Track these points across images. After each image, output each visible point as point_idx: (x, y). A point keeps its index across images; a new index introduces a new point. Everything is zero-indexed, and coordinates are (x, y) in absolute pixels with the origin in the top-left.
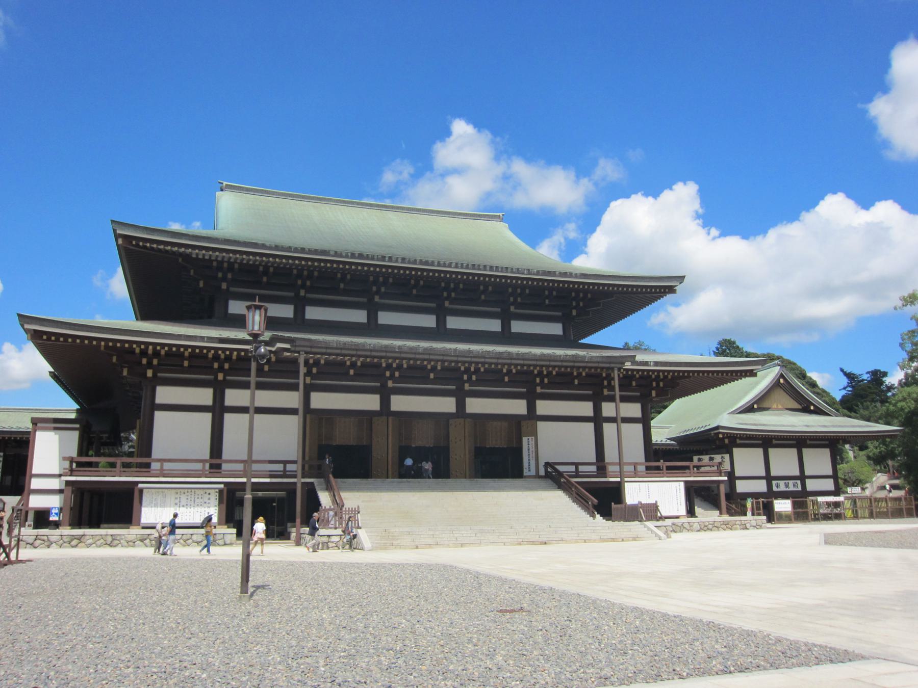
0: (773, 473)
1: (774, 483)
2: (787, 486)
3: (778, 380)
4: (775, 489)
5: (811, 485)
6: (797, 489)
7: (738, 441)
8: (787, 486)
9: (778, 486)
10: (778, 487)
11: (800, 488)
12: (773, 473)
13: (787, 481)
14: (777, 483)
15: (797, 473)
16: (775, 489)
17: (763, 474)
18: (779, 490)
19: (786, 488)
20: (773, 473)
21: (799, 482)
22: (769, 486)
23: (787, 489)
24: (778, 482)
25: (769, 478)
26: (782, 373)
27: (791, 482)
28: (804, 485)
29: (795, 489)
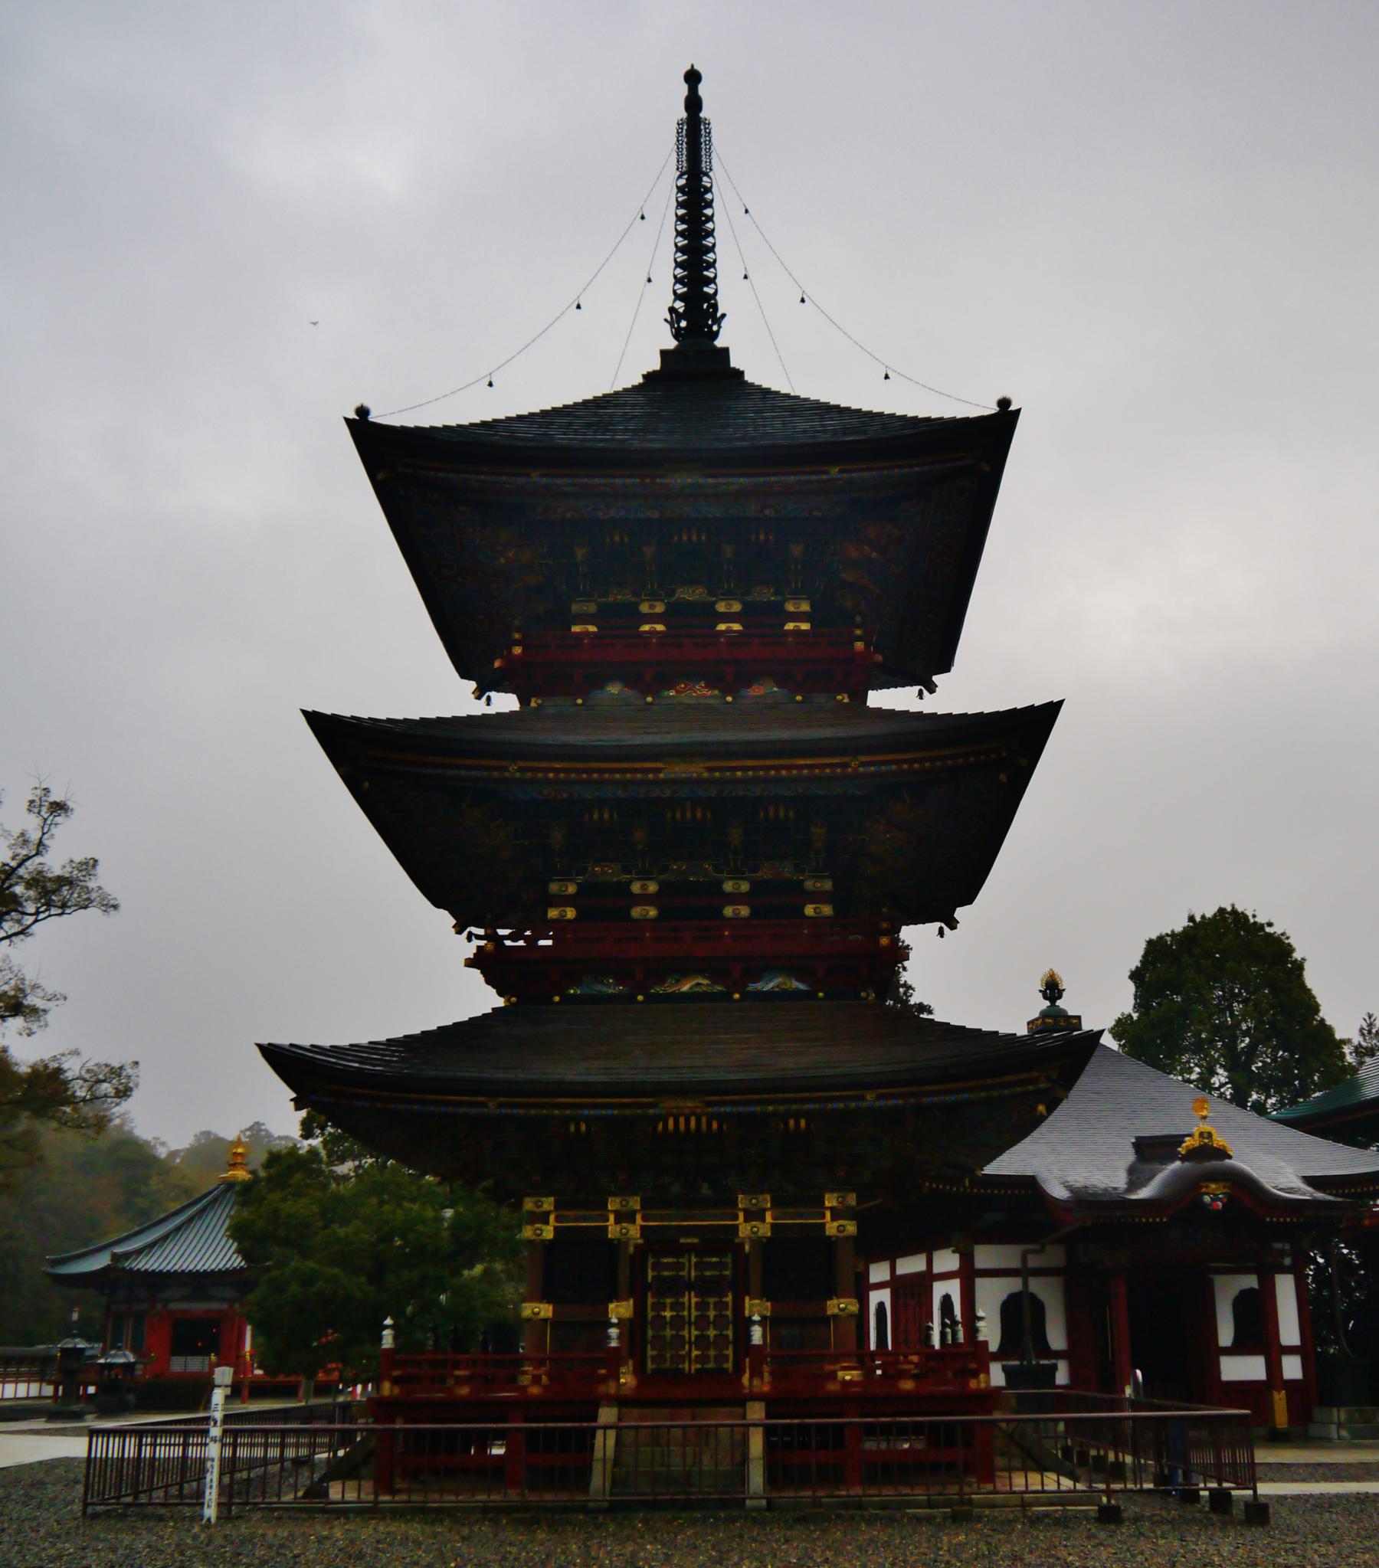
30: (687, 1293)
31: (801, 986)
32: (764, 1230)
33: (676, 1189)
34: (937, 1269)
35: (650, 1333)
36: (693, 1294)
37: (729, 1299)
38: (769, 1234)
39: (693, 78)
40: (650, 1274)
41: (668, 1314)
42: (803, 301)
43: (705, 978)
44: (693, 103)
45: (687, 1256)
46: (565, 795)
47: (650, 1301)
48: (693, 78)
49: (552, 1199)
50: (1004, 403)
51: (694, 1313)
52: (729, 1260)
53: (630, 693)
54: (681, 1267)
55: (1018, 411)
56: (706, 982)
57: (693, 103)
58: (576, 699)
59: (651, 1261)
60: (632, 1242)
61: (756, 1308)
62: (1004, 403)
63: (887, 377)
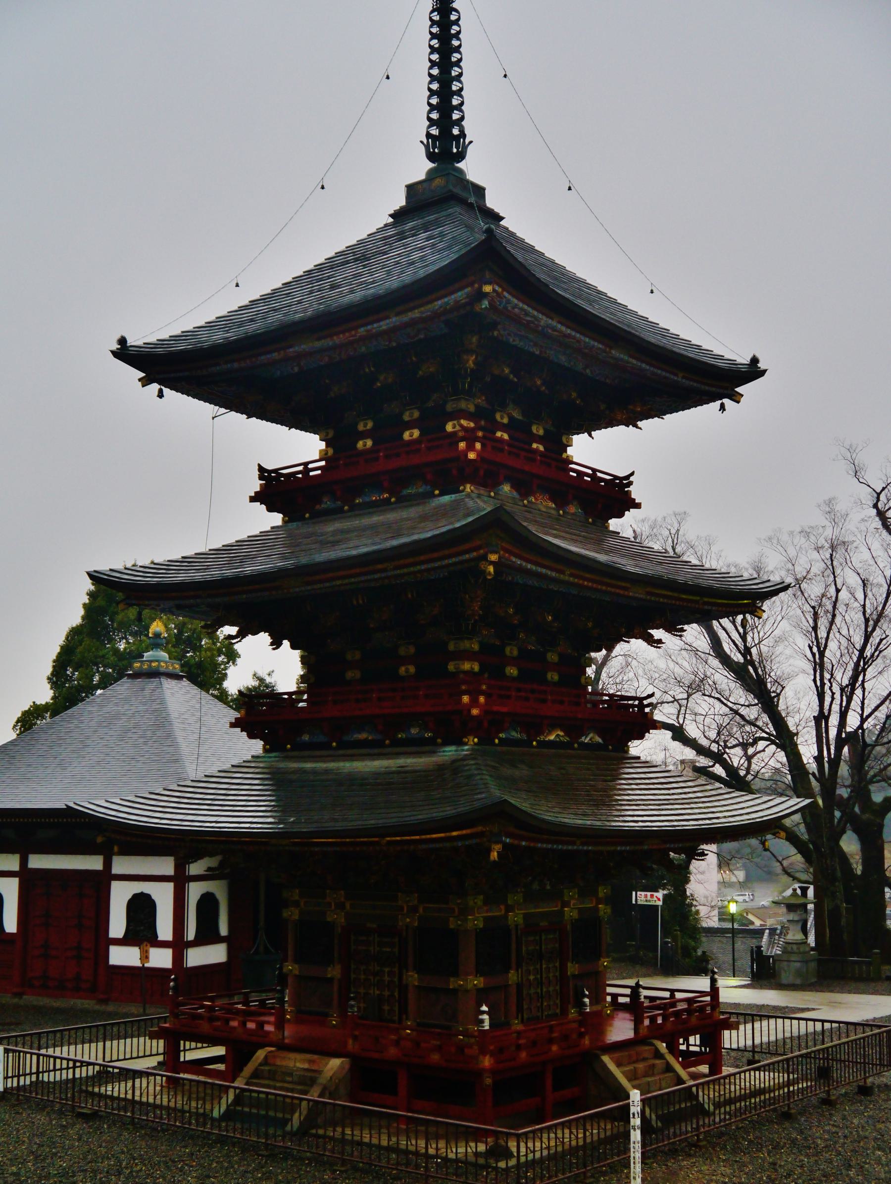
31: (600, 740)
33: (535, 886)
34: (116, 870)
35: (525, 992)
36: (543, 962)
37: (557, 964)
40: (524, 949)
42: (570, 189)
43: (562, 730)
46: (510, 578)
49: (481, 897)
50: (755, 361)
53: (515, 494)
55: (764, 372)
56: (561, 733)
58: (490, 492)
59: (524, 939)
62: (755, 361)
63: (652, 292)
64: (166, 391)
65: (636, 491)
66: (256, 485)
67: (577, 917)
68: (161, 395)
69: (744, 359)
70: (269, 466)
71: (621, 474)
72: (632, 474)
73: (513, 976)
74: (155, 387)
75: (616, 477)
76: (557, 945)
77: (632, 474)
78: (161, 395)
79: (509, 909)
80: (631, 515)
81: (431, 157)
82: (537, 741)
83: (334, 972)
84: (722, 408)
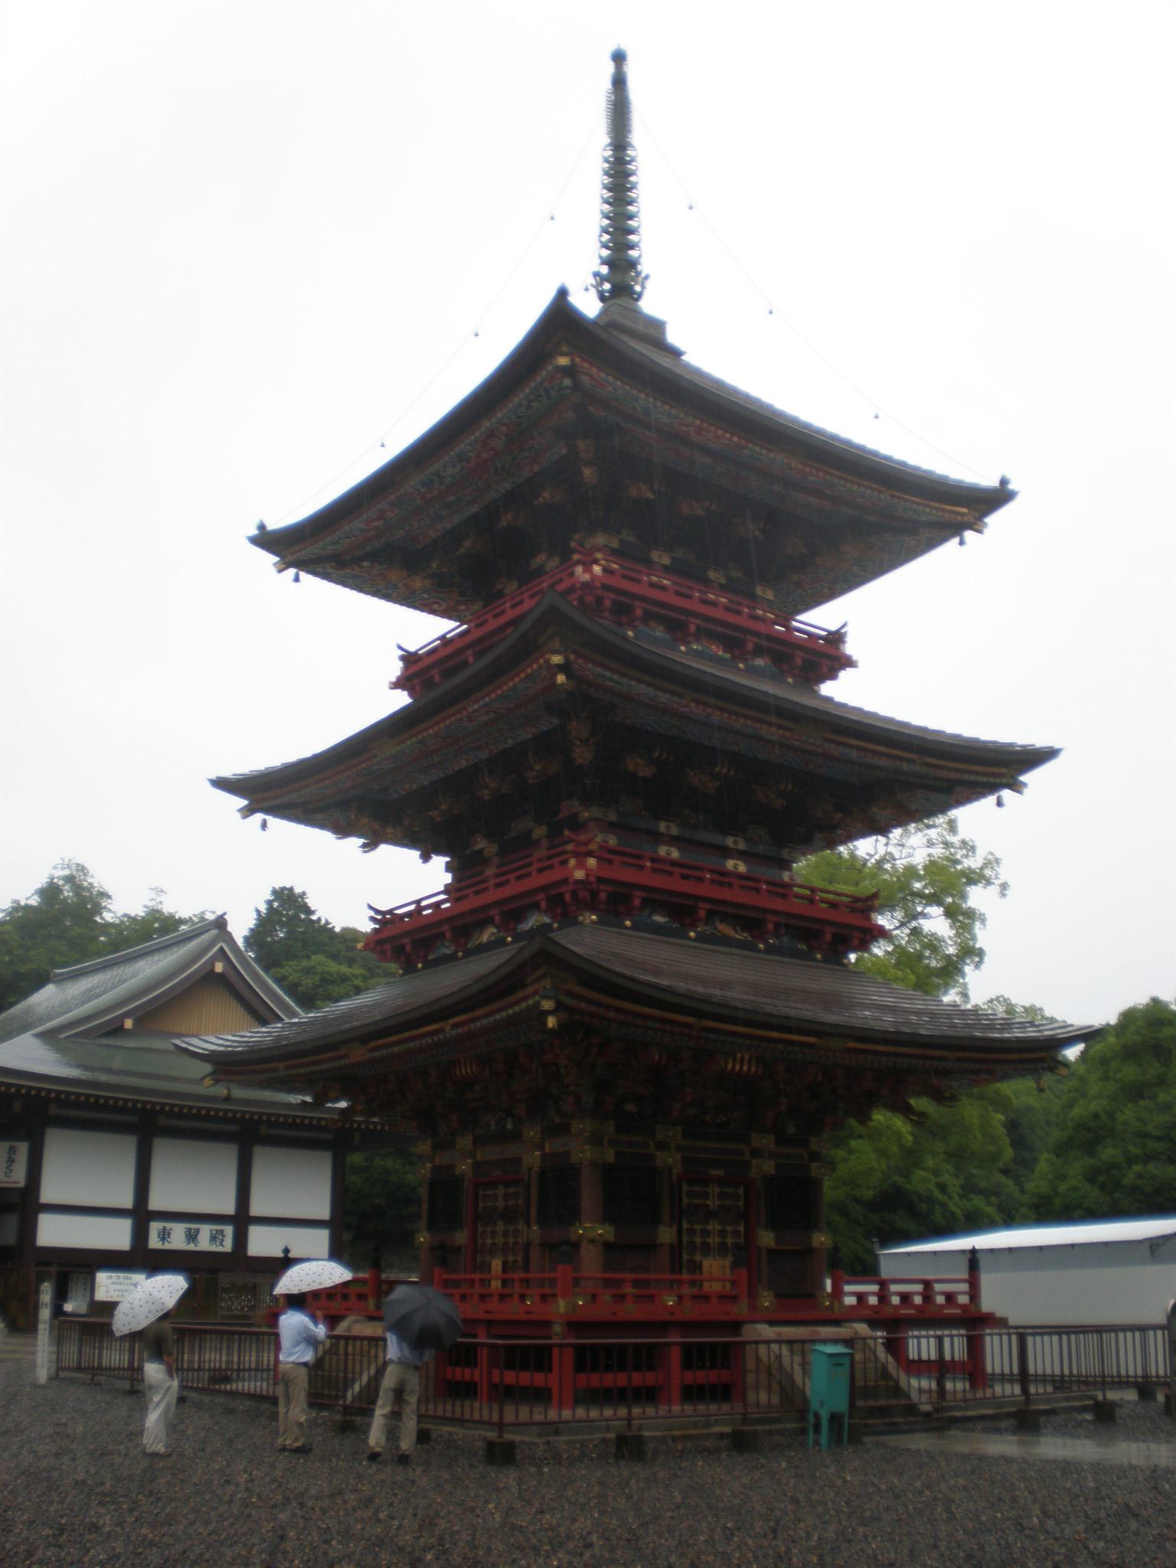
0: (156, 1203)
1: (155, 1227)
2: (192, 1236)
3: (212, 962)
4: (154, 1242)
5: (263, 1243)
6: (220, 1249)
7: (53, 1110)
8: (192, 1236)
9: (164, 1235)
10: (163, 1239)
11: (228, 1246)
12: (157, 1201)
13: (194, 1226)
14: (164, 1228)
15: (229, 1207)
16: (154, 1242)
17: (127, 1201)
18: (167, 1246)
19: (189, 1243)
20: (156, 1203)
21: (229, 1230)
22: (140, 1234)
23: (192, 1247)
24: (169, 1225)
25: (141, 1215)
26: (222, 949)
27: (205, 1230)
28: (241, 1239)
29: (214, 1248)
30: (711, 1222)
32: (769, 1167)
35: (685, 1257)
37: (741, 1228)
38: (773, 1172)
39: (619, 58)
40: (685, 1200)
41: (698, 1240)
44: (619, 83)
45: (711, 1185)
47: (685, 1225)
48: (619, 58)
50: (1004, 482)
51: (718, 1240)
52: (741, 1191)
54: (706, 1195)
57: (619, 83)
60: (674, 1171)
61: (767, 1238)
62: (1004, 482)
64: (302, 575)
65: (850, 648)
66: (396, 668)
67: (773, 1172)
68: (297, 579)
69: (990, 481)
70: (412, 648)
71: (833, 628)
72: (844, 626)
73: (666, 1235)
74: (292, 571)
75: (830, 633)
76: (741, 1204)
77: (844, 626)
78: (297, 579)
79: (662, 1146)
80: (845, 675)
81: (602, 298)
82: (698, 933)
83: (461, 1237)
84: (962, 543)
